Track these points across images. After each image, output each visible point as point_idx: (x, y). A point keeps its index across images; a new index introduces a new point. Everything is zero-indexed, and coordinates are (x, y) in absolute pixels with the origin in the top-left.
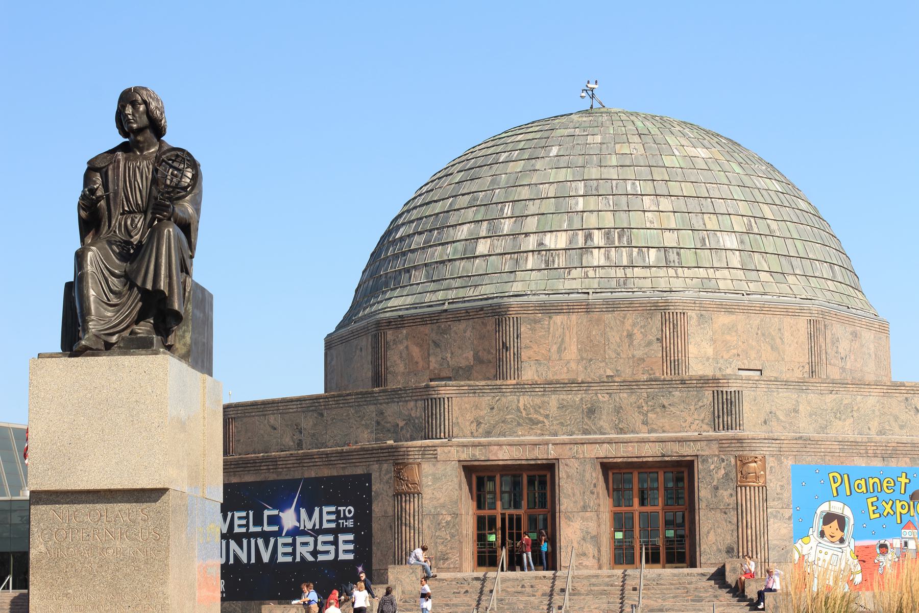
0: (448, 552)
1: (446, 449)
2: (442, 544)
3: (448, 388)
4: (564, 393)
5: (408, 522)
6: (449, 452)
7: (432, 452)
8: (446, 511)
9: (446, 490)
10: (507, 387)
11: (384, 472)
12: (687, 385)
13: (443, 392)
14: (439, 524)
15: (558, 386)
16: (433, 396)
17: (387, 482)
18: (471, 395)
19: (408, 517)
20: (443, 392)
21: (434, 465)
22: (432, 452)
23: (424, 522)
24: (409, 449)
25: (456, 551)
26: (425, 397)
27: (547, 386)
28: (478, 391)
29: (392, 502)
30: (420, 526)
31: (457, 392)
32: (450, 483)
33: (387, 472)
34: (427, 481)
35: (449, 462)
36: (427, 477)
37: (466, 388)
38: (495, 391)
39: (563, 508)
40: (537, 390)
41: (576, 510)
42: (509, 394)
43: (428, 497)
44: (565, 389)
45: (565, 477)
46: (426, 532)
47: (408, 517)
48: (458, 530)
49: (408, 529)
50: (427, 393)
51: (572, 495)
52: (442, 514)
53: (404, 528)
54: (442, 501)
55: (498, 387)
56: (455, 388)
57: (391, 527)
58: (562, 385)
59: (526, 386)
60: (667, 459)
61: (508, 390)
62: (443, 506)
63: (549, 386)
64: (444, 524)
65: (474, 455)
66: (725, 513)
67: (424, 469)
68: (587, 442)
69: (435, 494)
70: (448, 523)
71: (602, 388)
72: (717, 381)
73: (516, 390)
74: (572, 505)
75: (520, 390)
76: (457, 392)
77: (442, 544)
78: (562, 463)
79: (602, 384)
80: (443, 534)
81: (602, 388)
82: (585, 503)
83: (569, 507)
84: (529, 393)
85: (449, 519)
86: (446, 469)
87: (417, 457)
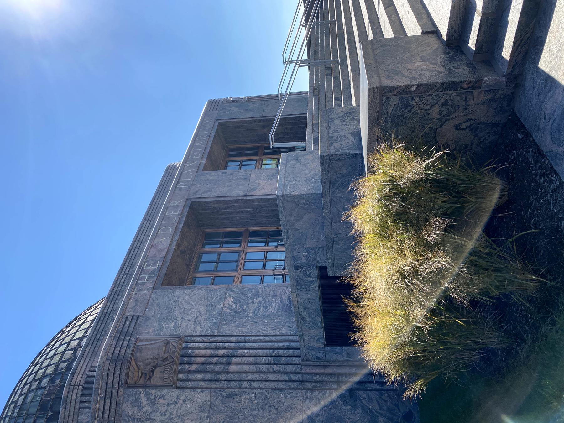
0: (279, 300)
1: (132, 303)
2: (266, 308)
3: (78, 371)
4: (136, 259)
5: (224, 360)
6: (136, 300)
7: (128, 323)
8: (219, 303)
9: (189, 303)
10: (107, 307)
11: (136, 410)
12: (166, 183)
13: (79, 377)
14: (236, 312)
15: (127, 263)
16: (80, 392)
17: (153, 403)
18: (99, 344)
19: (215, 360)
20: (79, 377)
21: (148, 319)
22: (128, 323)
23: (228, 333)
24: (110, 354)
25: (279, 291)
26: (77, 407)
27: (123, 272)
28: (98, 336)
29: (188, 393)
30: (233, 339)
31: (87, 360)
32: (180, 300)
33: (137, 404)
34: (168, 328)
35: (151, 300)
36: (161, 329)
37: (88, 349)
38: (106, 319)
39: (242, 193)
40: (123, 280)
41: (247, 185)
42: (115, 306)
43: (193, 327)
44: (133, 258)
45: (208, 193)
46: (245, 330)
47: (215, 360)
48: (250, 289)
49: (235, 360)
50: (73, 402)
51: (230, 188)
52: (222, 309)
53: (233, 368)
54: (202, 309)
55: (103, 316)
56: (82, 362)
57: (229, 396)
58: (128, 261)
59: (115, 290)
60: (213, 134)
61: (111, 306)
62: (210, 307)
63: (124, 270)
64: (238, 305)
65: (153, 273)
66: (269, 105)
67: (148, 333)
68: (178, 179)
69: (189, 317)
70: (236, 301)
71: (145, 232)
72: (170, 169)
73: (115, 299)
74: (240, 187)
75: (116, 295)
76: (87, 360)
77: (266, 308)
78: (192, 196)
79: (141, 232)
80: (252, 307)
81: (145, 232)
82: (241, 179)
83: (243, 189)
84: (123, 287)
85: (231, 299)
86: (159, 305)
87: (126, 343)
